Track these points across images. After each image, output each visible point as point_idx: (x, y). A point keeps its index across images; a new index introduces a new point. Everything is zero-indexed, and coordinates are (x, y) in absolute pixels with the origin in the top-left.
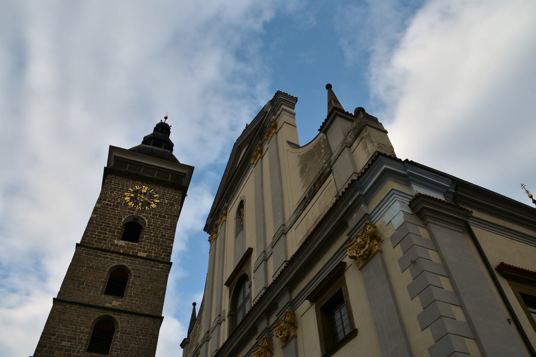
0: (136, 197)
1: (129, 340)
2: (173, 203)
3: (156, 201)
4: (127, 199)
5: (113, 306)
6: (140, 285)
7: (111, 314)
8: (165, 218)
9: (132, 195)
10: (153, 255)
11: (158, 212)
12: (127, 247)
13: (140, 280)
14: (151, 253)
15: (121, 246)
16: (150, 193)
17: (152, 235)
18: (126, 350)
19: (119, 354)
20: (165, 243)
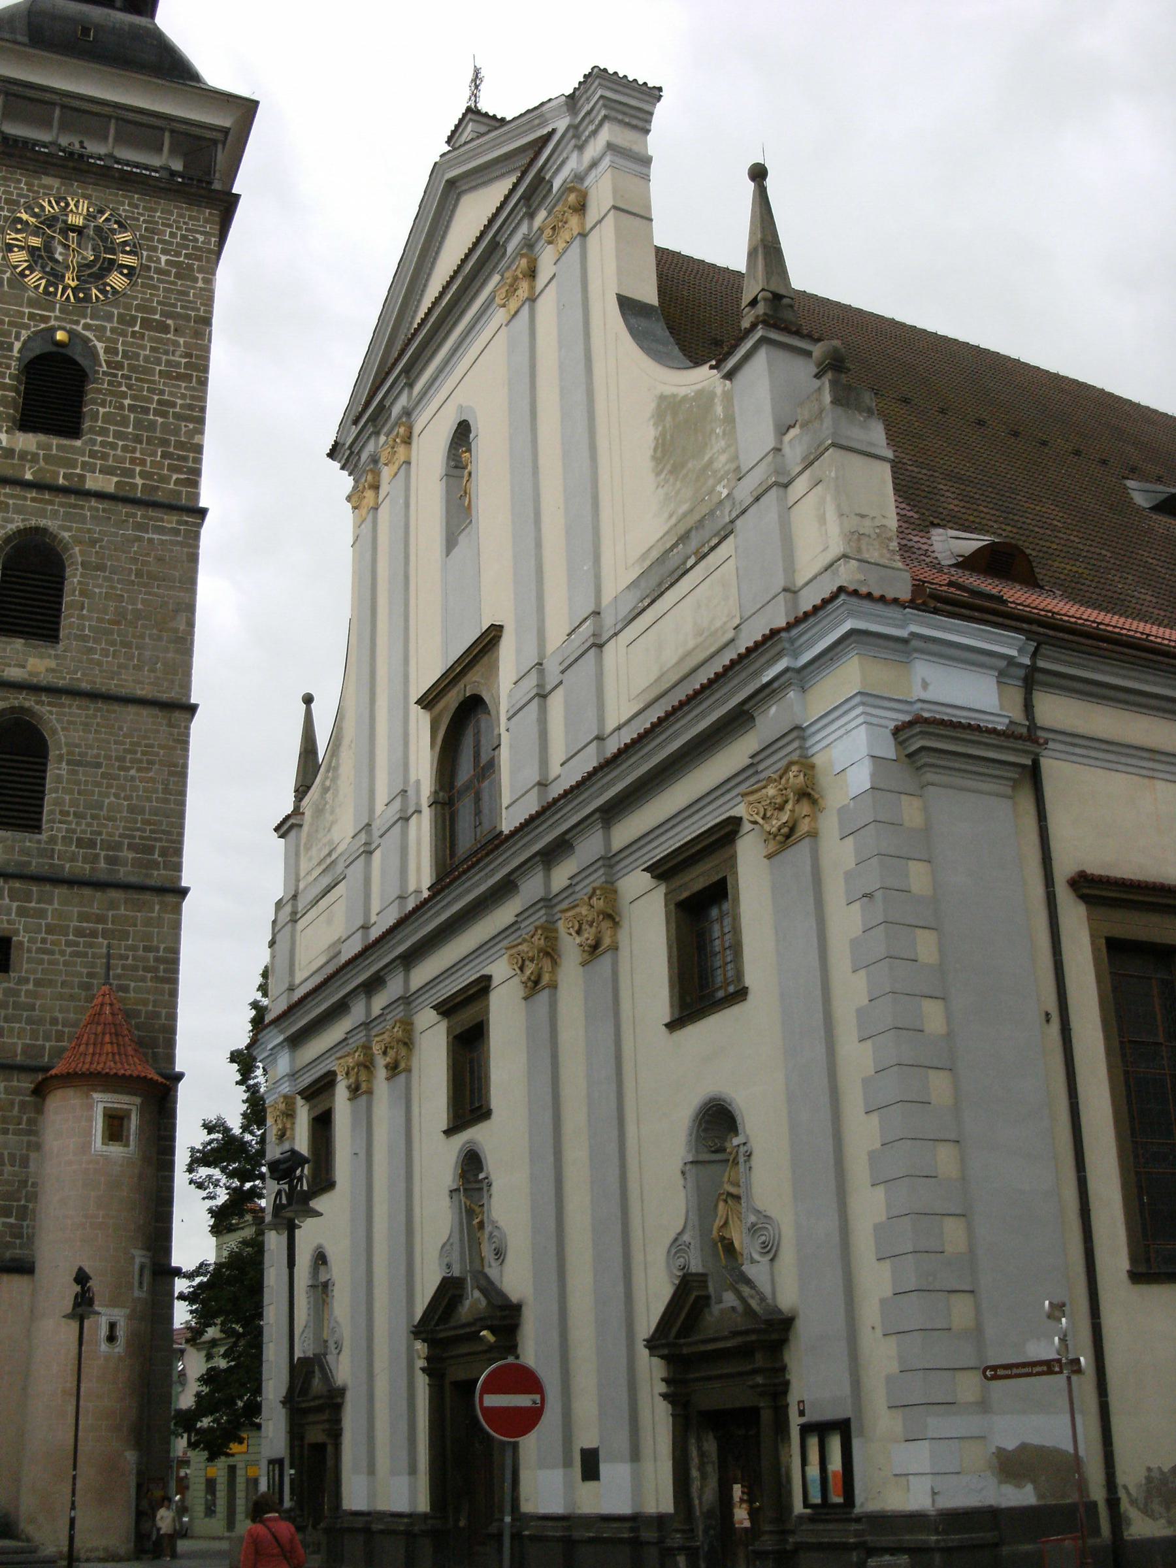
0: (48, 247)
1: (98, 784)
2: (190, 267)
3: (124, 259)
4: (19, 257)
5: (30, 674)
6: (107, 596)
8: (165, 329)
9: (35, 241)
10: (139, 481)
11: (139, 308)
12: (47, 458)
13: (106, 579)
14: (130, 473)
15: (23, 455)
16: (98, 229)
17: (127, 402)
18: (94, 817)
19: (74, 831)
20: (176, 432)
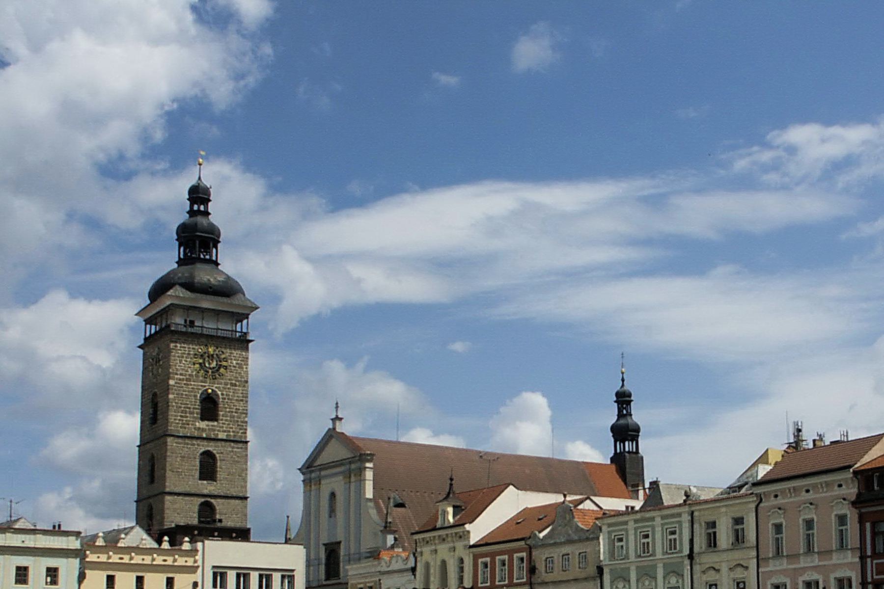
7: (209, 499)
8: (236, 385)
